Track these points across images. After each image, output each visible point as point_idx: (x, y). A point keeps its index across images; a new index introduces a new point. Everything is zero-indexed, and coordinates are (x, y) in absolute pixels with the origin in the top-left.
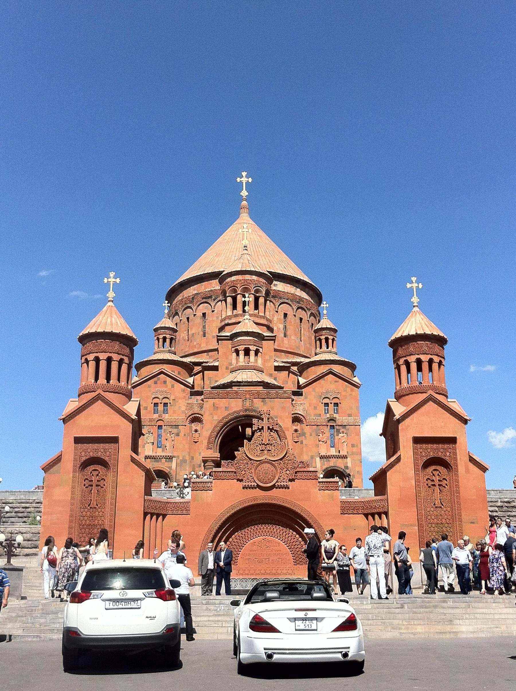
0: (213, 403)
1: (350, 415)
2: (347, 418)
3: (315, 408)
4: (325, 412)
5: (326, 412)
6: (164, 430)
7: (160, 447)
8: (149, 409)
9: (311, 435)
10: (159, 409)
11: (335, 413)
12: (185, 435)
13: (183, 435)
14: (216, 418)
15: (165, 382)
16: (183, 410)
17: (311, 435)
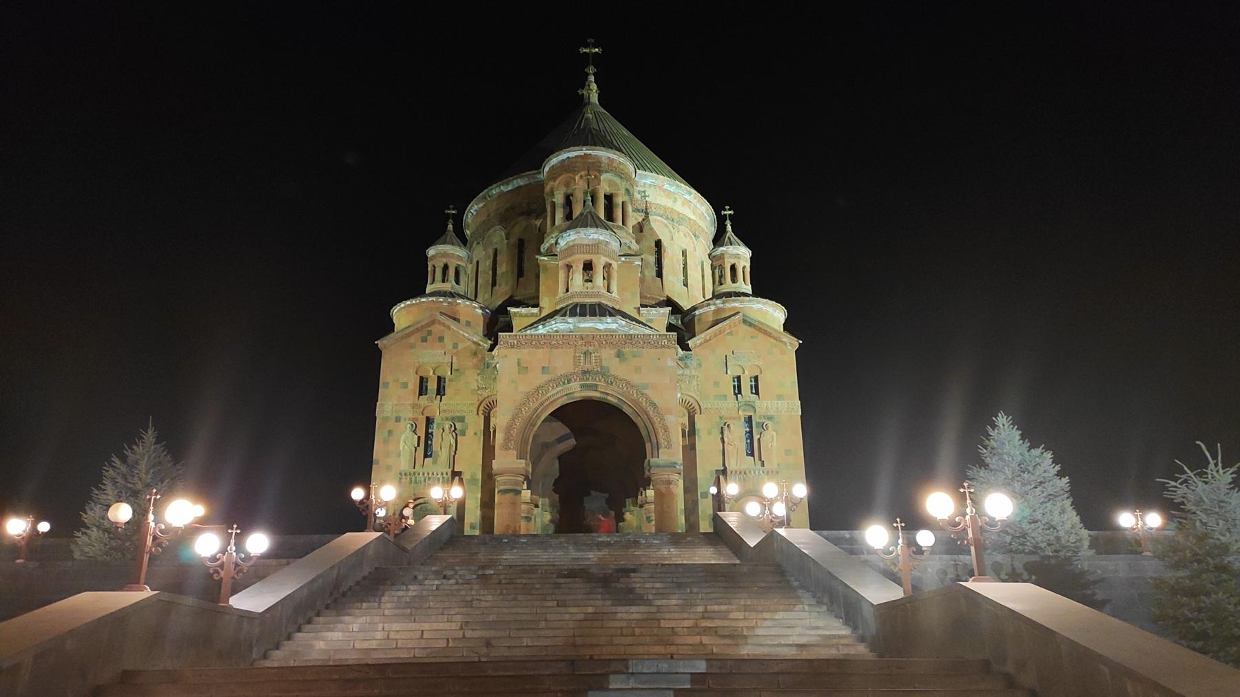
0: (518, 359)
1: (780, 397)
2: (776, 402)
3: (717, 384)
4: (734, 392)
5: (736, 392)
6: (438, 424)
7: (431, 456)
8: (411, 386)
9: (709, 433)
10: (428, 388)
11: (752, 393)
12: (475, 434)
13: (472, 434)
14: (524, 388)
15: (441, 339)
16: (473, 388)
17: (709, 433)
